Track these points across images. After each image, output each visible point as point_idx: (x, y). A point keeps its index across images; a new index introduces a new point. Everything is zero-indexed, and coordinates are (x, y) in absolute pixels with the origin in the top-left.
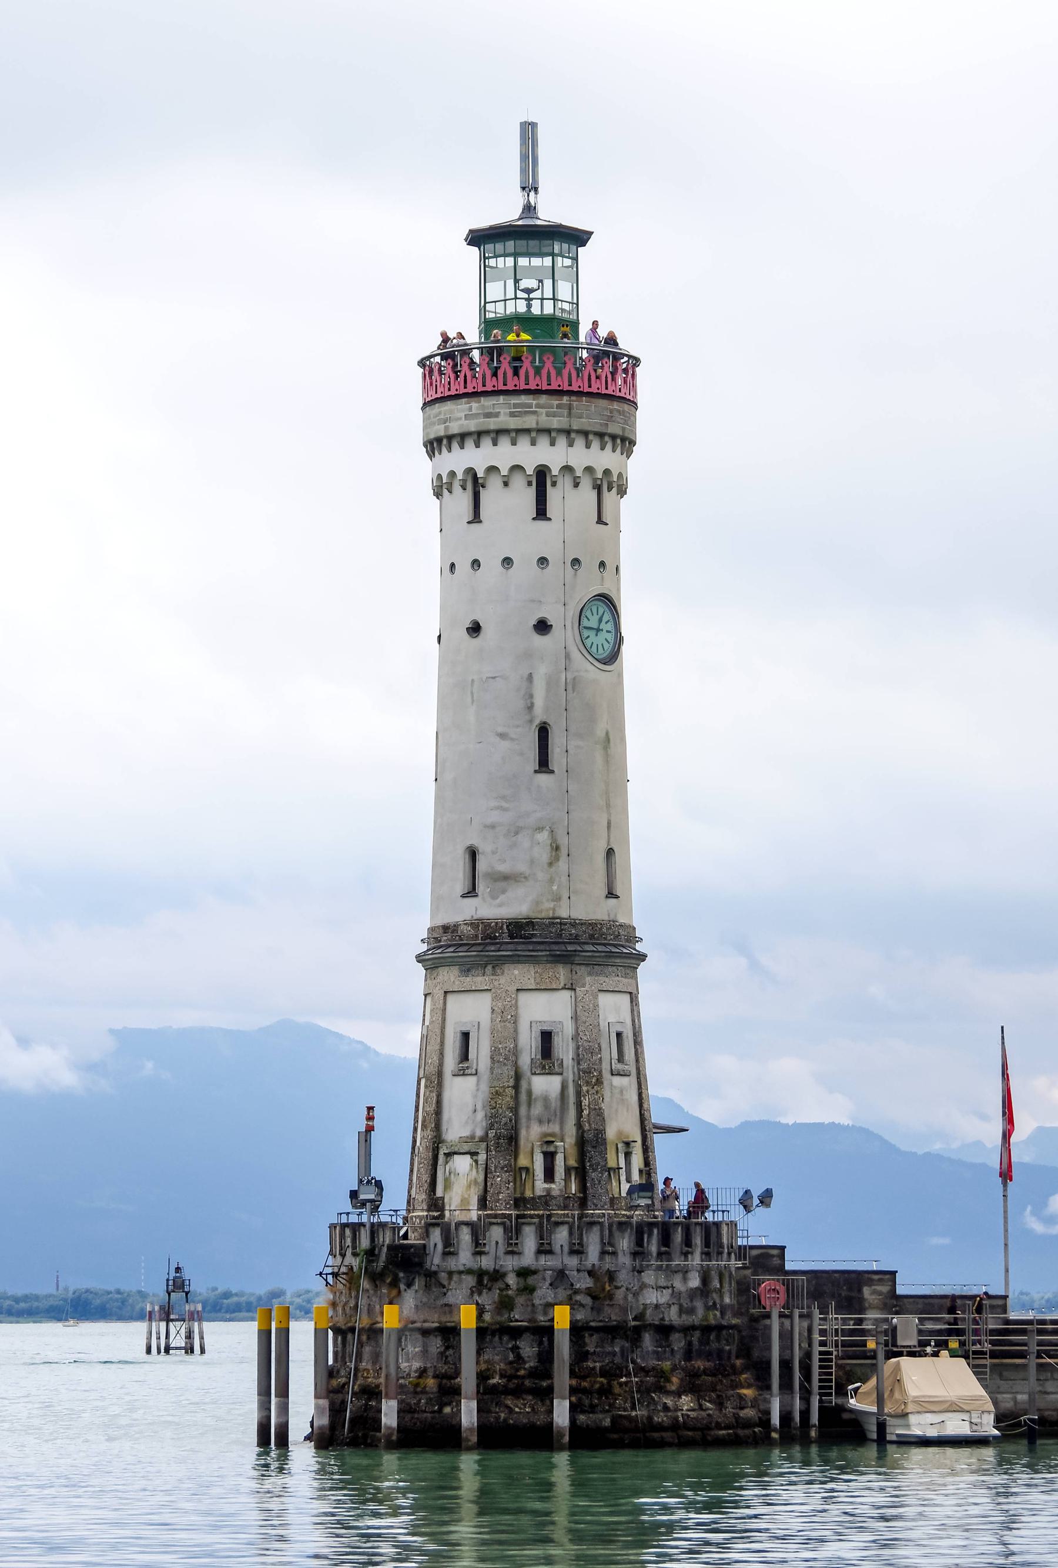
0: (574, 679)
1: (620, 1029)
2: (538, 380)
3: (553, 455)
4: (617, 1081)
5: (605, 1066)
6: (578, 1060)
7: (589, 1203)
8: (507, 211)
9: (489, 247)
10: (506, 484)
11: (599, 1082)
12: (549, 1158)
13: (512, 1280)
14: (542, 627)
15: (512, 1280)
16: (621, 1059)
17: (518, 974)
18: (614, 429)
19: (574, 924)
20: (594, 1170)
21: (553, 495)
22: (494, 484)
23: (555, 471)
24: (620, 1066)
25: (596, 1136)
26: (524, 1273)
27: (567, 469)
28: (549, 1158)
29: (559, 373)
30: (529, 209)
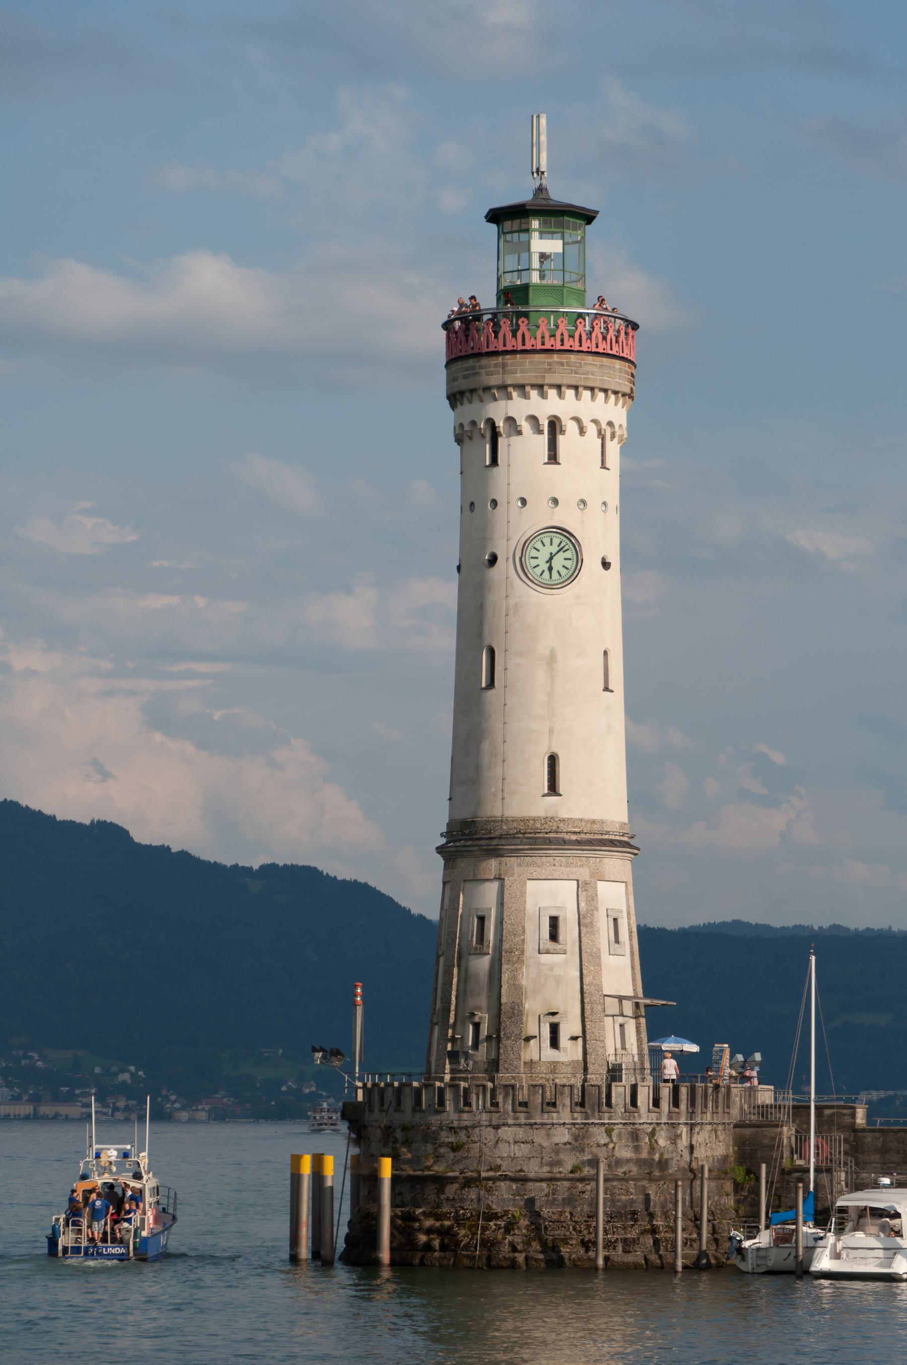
0: (516, 604)
1: (554, 914)
2: (552, 341)
3: (498, 410)
4: (545, 958)
5: (530, 947)
6: (500, 940)
7: (501, 1067)
8: (523, 195)
9: (507, 225)
10: (471, 438)
11: (520, 960)
12: (477, 1026)
13: (399, 1134)
14: (493, 560)
15: (399, 1134)
16: (554, 937)
17: (463, 864)
18: (549, 379)
19: (503, 820)
20: (508, 1038)
21: (502, 442)
22: (466, 440)
23: (500, 424)
24: (551, 945)
25: (513, 1008)
26: (405, 1129)
27: (510, 420)
28: (477, 1026)
29: (514, 335)
30: (540, 190)
